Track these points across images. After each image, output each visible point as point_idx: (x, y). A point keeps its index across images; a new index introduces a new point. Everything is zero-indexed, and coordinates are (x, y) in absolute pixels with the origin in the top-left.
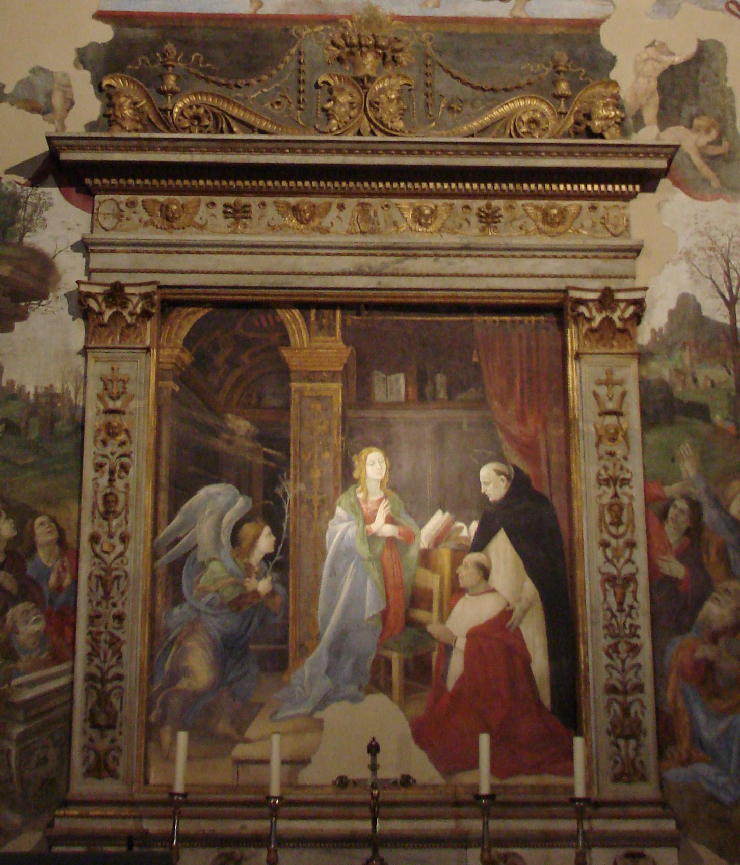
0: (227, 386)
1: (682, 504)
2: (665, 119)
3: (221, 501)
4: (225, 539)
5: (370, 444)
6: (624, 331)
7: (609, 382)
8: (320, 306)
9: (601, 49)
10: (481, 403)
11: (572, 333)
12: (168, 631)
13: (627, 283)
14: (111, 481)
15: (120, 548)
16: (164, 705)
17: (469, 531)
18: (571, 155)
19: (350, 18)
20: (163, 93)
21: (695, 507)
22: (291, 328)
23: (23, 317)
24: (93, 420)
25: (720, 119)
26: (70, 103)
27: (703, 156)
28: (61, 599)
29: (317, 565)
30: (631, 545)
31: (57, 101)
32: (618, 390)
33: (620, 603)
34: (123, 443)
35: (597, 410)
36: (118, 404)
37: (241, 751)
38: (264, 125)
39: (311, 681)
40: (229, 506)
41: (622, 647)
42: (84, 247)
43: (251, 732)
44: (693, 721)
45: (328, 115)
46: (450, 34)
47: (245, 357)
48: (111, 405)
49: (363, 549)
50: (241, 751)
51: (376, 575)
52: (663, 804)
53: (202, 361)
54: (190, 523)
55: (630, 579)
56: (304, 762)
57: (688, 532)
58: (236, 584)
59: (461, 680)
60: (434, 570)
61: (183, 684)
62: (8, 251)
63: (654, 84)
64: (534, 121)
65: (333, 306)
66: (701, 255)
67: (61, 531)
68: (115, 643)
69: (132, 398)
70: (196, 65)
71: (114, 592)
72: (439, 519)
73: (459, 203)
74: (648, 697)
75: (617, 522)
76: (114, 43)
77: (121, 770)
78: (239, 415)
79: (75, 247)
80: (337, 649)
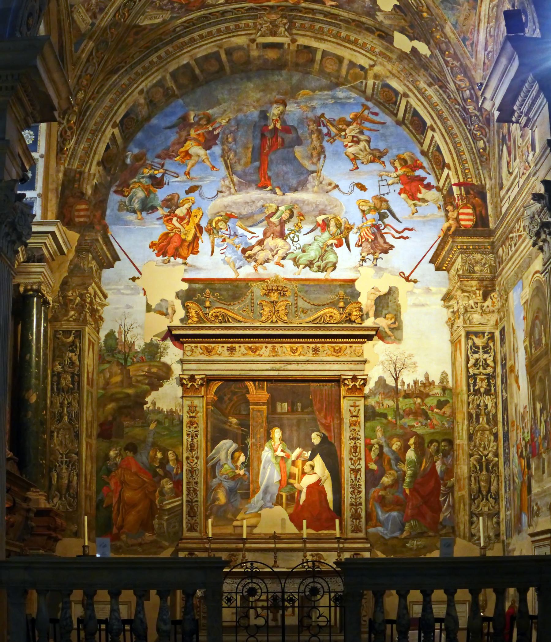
0: (229, 408)
1: (377, 446)
2: (376, 316)
3: (228, 445)
4: (229, 457)
5: (276, 426)
6: (360, 389)
7: (354, 406)
8: (259, 381)
9: (355, 290)
10: (312, 412)
11: (343, 389)
12: (211, 487)
13: (361, 373)
14: (192, 440)
15: (196, 461)
16: (211, 509)
17: (308, 454)
18: (343, 330)
19: (269, 279)
20: (206, 307)
21: (381, 447)
22: (250, 388)
23: (162, 386)
24: (186, 420)
25: (395, 315)
26: (174, 312)
27: (389, 328)
28: (178, 477)
29: (259, 466)
30: (360, 459)
31: (170, 311)
32: (357, 408)
33: (356, 478)
34: (195, 427)
35: (350, 415)
36: (194, 414)
37: (235, 523)
38: (240, 319)
39: (258, 501)
40: (230, 446)
41: (356, 491)
42: (182, 362)
43: (239, 518)
44: (377, 514)
45: (262, 315)
46: (303, 285)
47: (235, 398)
48: (191, 415)
49: (274, 460)
50: (235, 523)
51: (278, 469)
52: (367, 539)
53: (221, 399)
54: (218, 452)
55: (359, 470)
56: (255, 526)
57: (378, 455)
58: (233, 472)
59: (304, 501)
60: (296, 467)
61: (217, 503)
62: (156, 364)
63: (373, 303)
64: (331, 316)
65: (264, 381)
66: (387, 363)
67: (177, 456)
68: (195, 491)
69: (198, 412)
70: (216, 297)
71: (194, 475)
72: (298, 451)
73: (306, 345)
74: (363, 507)
75: (356, 452)
76: (189, 290)
77: (198, 529)
78: (233, 417)
79: (178, 362)
80: (266, 492)
